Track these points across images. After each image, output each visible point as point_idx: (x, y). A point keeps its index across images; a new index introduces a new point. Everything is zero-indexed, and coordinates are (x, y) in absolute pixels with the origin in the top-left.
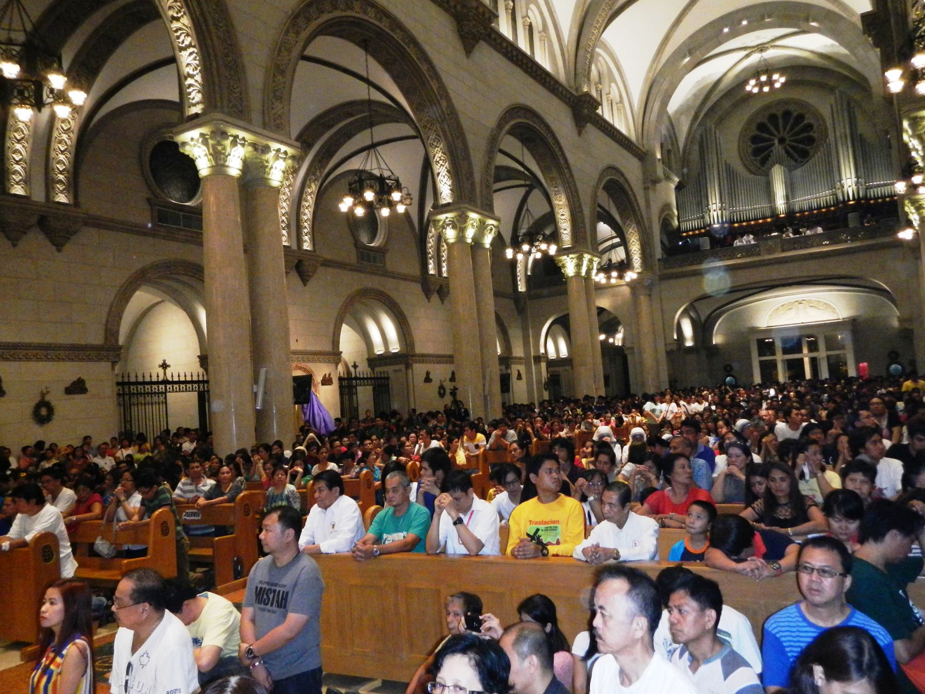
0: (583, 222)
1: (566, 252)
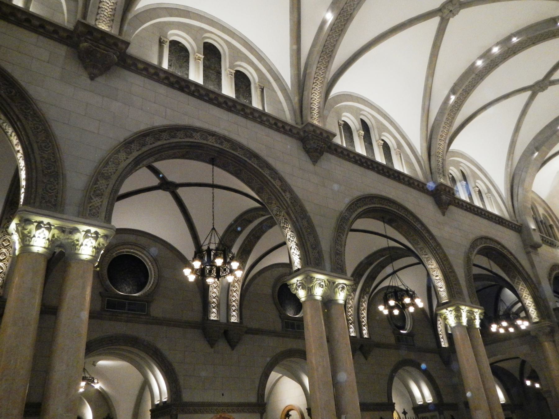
0: (457, 279)
1: (445, 306)
